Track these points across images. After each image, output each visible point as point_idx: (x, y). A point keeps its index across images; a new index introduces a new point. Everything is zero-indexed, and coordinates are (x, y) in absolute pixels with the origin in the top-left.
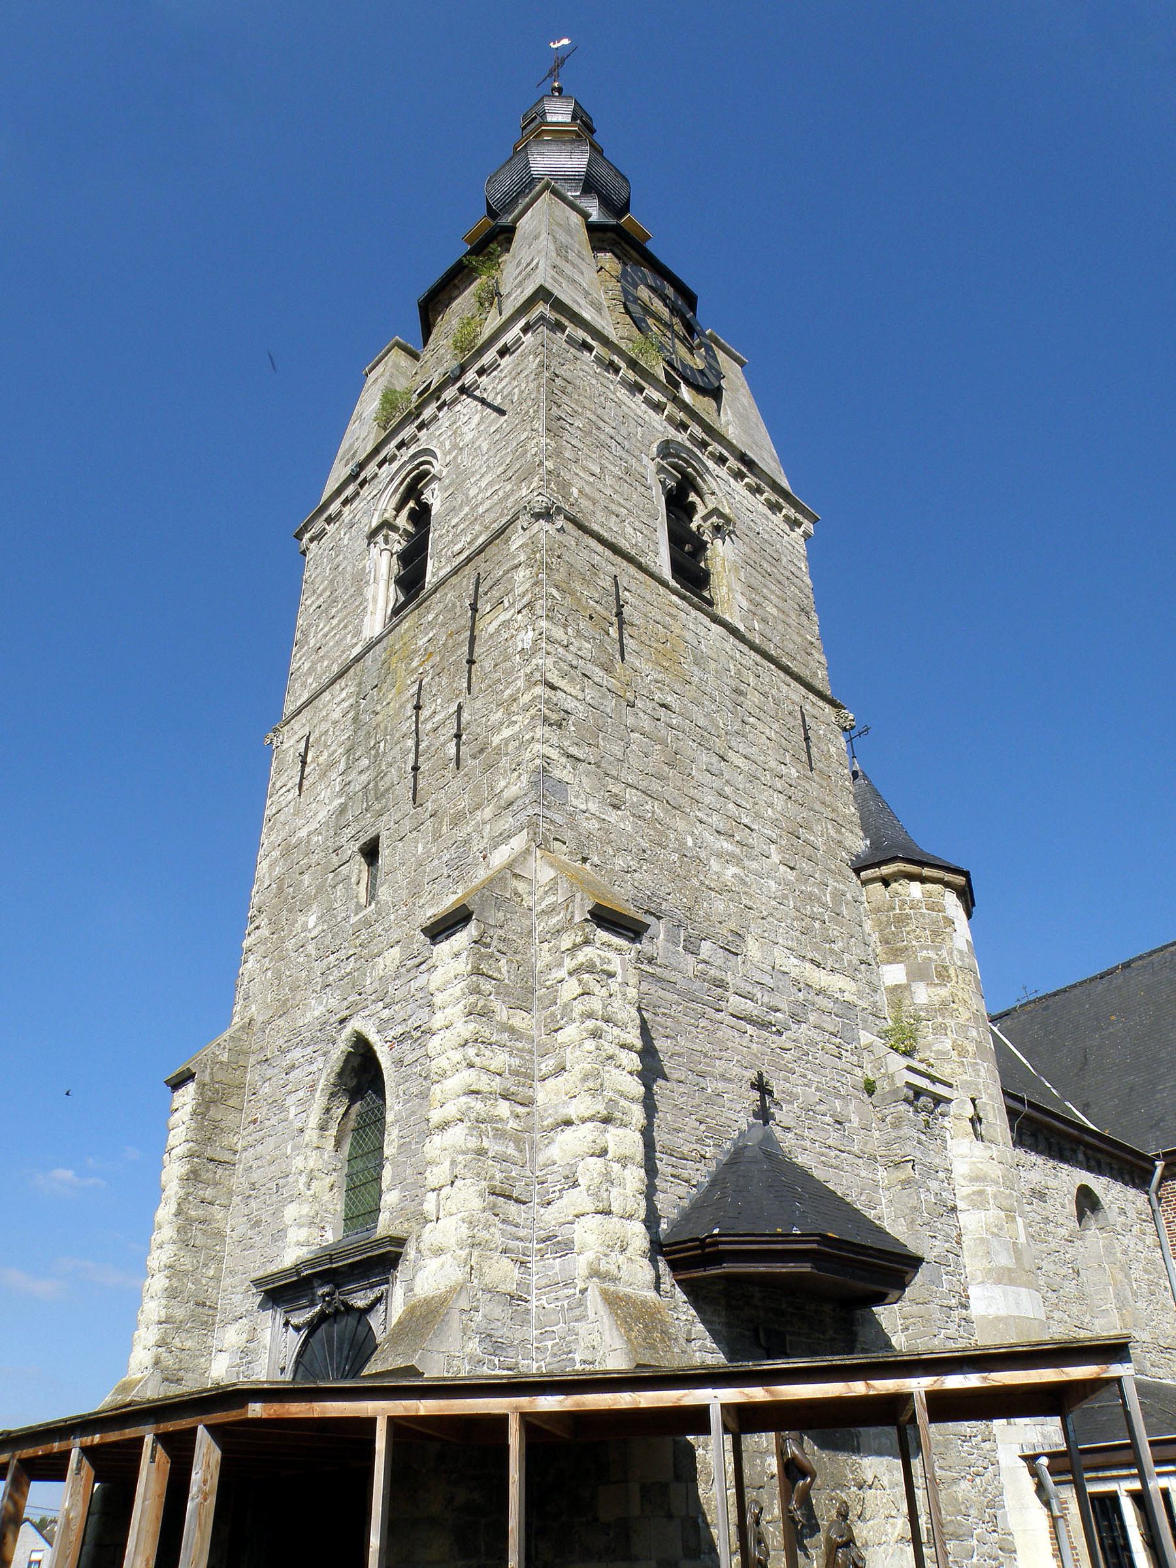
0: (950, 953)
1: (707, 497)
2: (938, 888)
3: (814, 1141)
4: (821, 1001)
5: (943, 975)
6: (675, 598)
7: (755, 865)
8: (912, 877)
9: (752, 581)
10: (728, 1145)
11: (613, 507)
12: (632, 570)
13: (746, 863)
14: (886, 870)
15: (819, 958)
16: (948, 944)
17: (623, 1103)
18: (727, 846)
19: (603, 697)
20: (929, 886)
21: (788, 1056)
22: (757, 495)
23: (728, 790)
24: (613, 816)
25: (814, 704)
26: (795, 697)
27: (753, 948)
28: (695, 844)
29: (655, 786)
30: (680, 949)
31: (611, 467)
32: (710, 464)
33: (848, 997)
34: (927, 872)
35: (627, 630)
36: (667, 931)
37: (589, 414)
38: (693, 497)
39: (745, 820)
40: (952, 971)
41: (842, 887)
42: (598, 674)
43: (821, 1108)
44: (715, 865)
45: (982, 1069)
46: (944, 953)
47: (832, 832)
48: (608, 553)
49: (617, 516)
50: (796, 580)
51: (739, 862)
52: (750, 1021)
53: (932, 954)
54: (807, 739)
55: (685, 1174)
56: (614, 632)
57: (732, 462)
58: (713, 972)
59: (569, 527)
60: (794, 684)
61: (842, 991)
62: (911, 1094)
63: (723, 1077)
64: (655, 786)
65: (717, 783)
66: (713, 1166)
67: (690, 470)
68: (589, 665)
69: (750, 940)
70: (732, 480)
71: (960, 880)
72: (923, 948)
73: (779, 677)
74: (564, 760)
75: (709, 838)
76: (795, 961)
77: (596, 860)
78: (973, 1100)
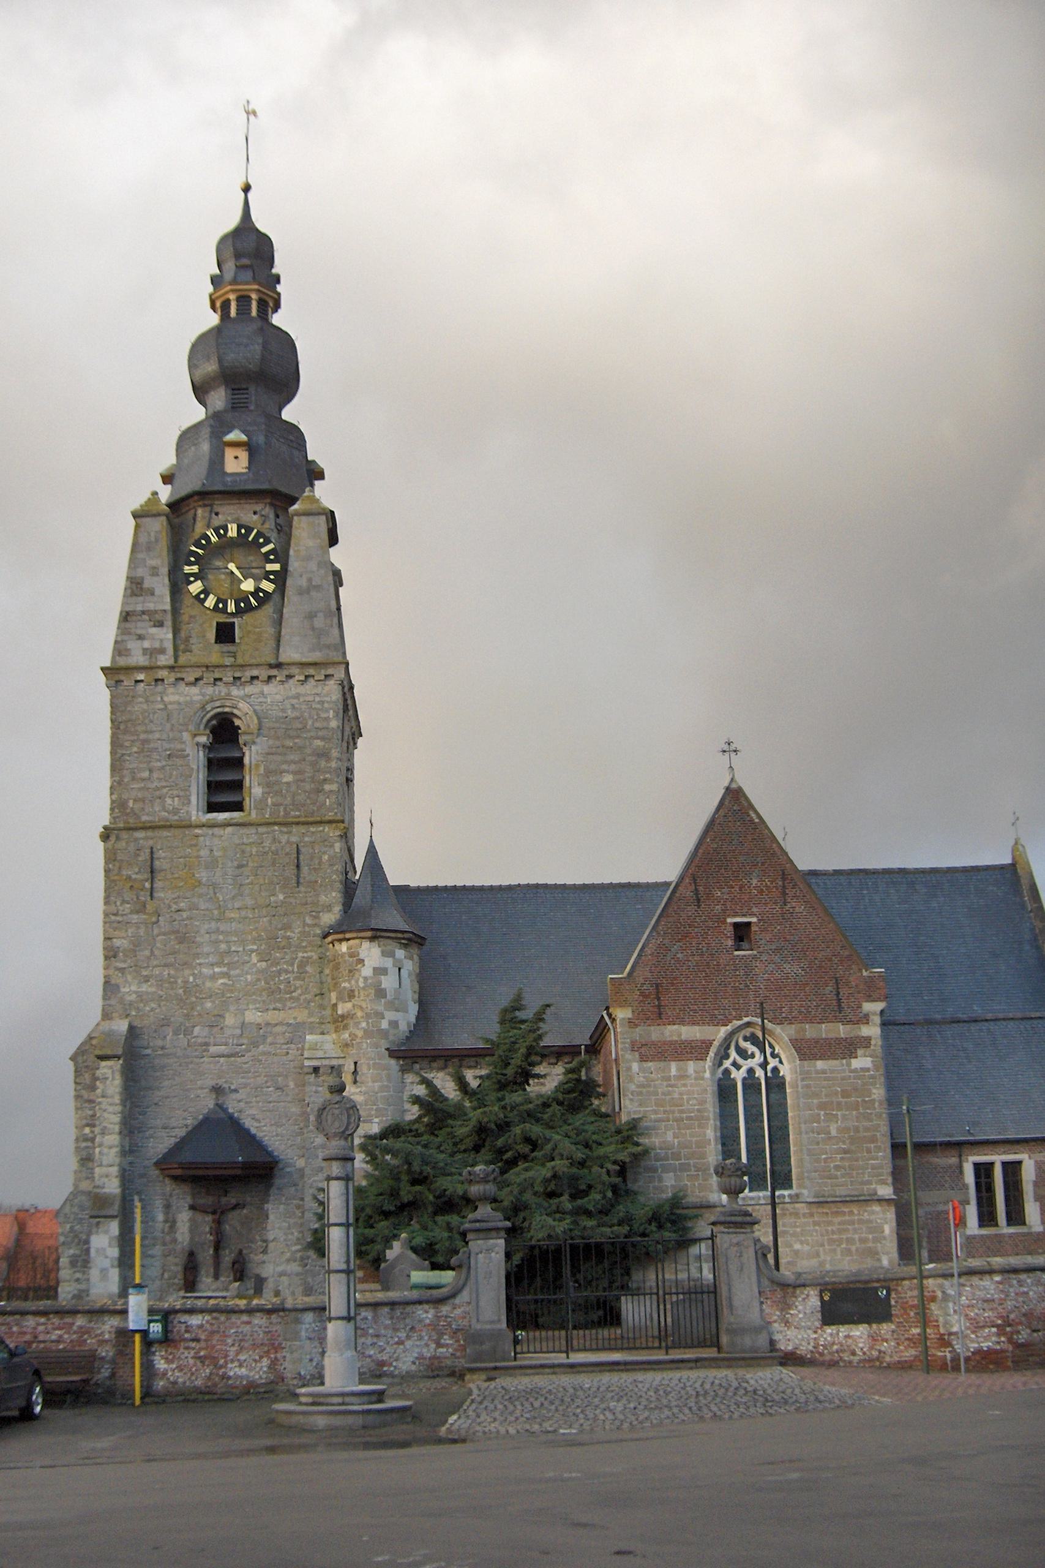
0: (357, 982)
1: (243, 718)
2: (357, 941)
3: (258, 1102)
4: (279, 1029)
5: (351, 995)
6: (198, 831)
7: (238, 971)
8: (340, 941)
9: (272, 767)
10: (201, 1117)
11: (158, 793)
12: (165, 833)
13: (232, 973)
14: (330, 939)
15: (279, 1005)
16: (357, 976)
17: (111, 1126)
18: (217, 970)
19: (138, 928)
20: (351, 942)
21: (247, 1066)
22: (291, 681)
23: (221, 937)
24: (145, 988)
25: (313, 833)
26: (294, 839)
27: (230, 1020)
28: (195, 979)
29: (171, 959)
30: (182, 1036)
31: (159, 764)
32: (249, 689)
33: (298, 1020)
34: (348, 936)
35: (159, 876)
36: (173, 1031)
37: (143, 736)
38: (237, 722)
39: (233, 949)
40: (356, 993)
41: (309, 954)
42: (135, 918)
43: (268, 1084)
44: (208, 984)
45: (365, 1045)
46: (353, 982)
47: (308, 921)
48: (150, 833)
49: (160, 798)
50: (320, 733)
51: (226, 975)
52: (223, 1056)
53: (346, 985)
54: (298, 866)
55: (174, 1134)
56: (147, 885)
57: (263, 673)
58: (200, 1040)
59: (124, 835)
60: (295, 829)
61: (295, 1018)
62: (311, 1070)
63: (202, 1088)
64: (171, 959)
65: (214, 937)
66: (190, 1128)
67: (227, 710)
68: (130, 916)
69: (227, 1015)
70: (266, 689)
71: (369, 934)
72: (345, 981)
73: (281, 832)
74: (116, 973)
75: (205, 970)
76: (260, 1014)
77: (134, 1013)
78: (356, 1063)
